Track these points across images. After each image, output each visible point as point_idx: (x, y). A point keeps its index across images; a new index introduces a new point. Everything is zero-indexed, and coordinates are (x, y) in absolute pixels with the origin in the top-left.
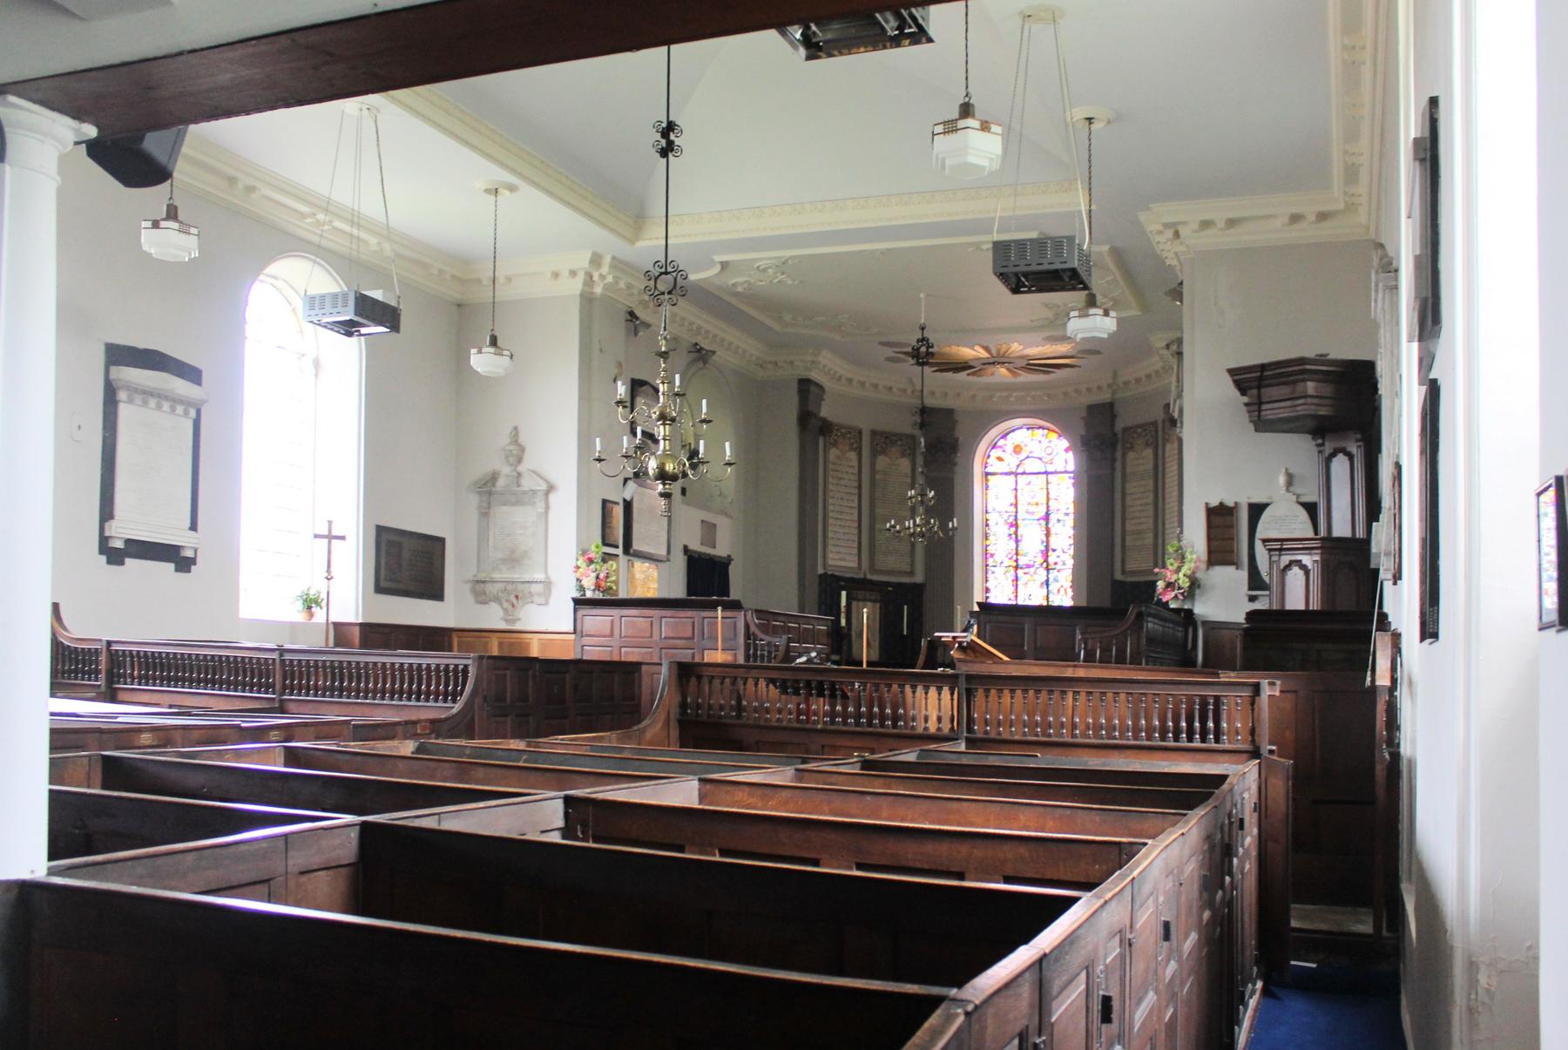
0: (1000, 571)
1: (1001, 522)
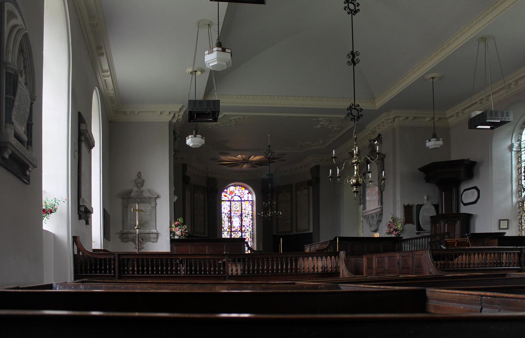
1: (226, 217)
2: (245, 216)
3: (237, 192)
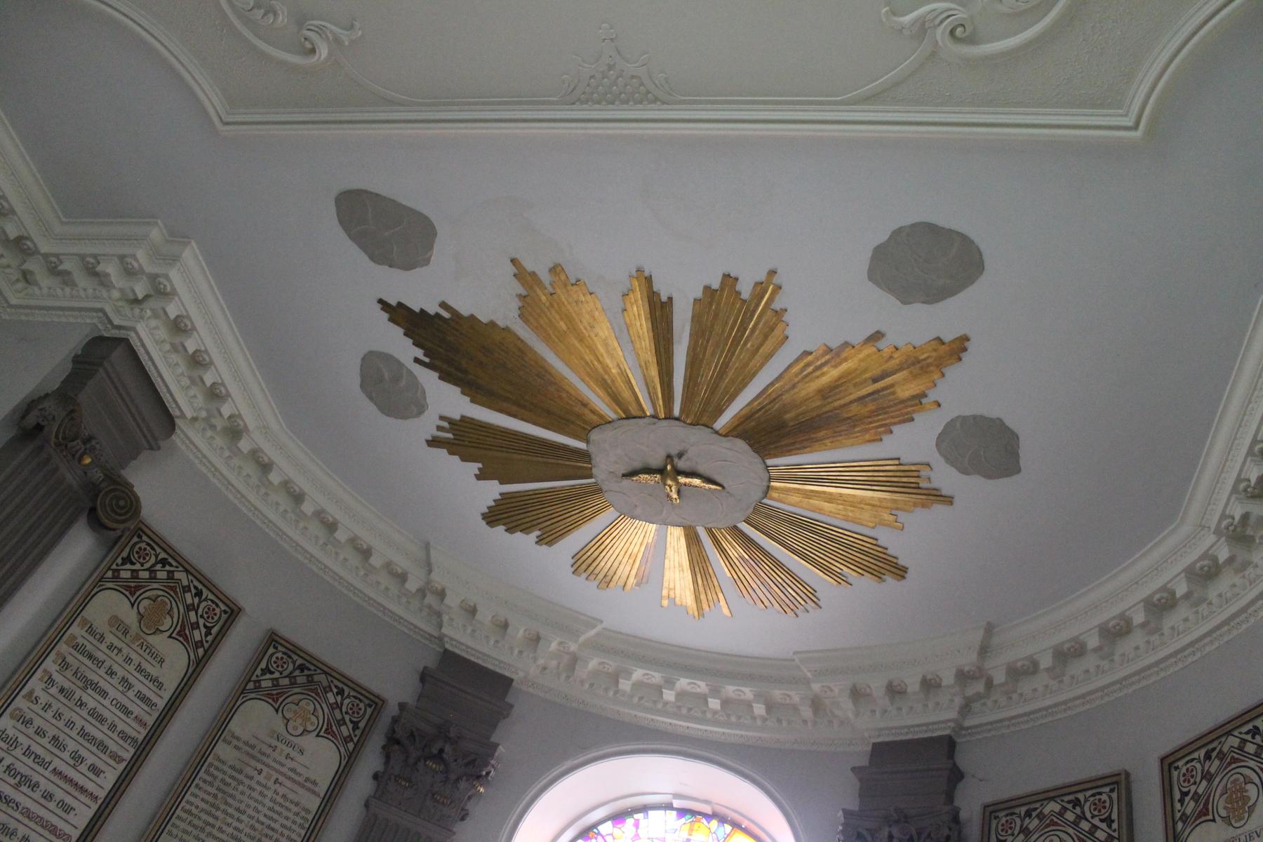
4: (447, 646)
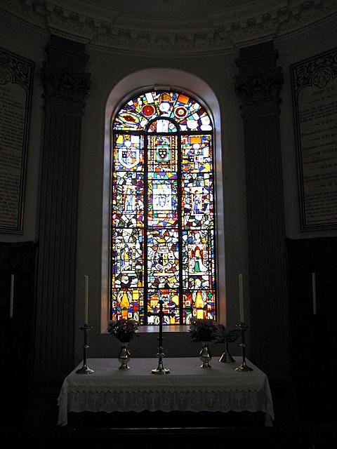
0: (127, 232)
1: (129, 181)
2: (191, 180)
3: (165, 107)
4: (53, 33)
